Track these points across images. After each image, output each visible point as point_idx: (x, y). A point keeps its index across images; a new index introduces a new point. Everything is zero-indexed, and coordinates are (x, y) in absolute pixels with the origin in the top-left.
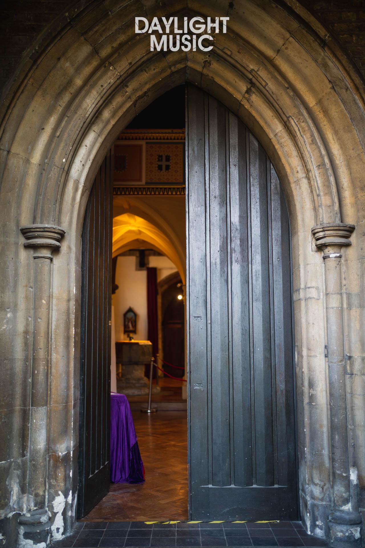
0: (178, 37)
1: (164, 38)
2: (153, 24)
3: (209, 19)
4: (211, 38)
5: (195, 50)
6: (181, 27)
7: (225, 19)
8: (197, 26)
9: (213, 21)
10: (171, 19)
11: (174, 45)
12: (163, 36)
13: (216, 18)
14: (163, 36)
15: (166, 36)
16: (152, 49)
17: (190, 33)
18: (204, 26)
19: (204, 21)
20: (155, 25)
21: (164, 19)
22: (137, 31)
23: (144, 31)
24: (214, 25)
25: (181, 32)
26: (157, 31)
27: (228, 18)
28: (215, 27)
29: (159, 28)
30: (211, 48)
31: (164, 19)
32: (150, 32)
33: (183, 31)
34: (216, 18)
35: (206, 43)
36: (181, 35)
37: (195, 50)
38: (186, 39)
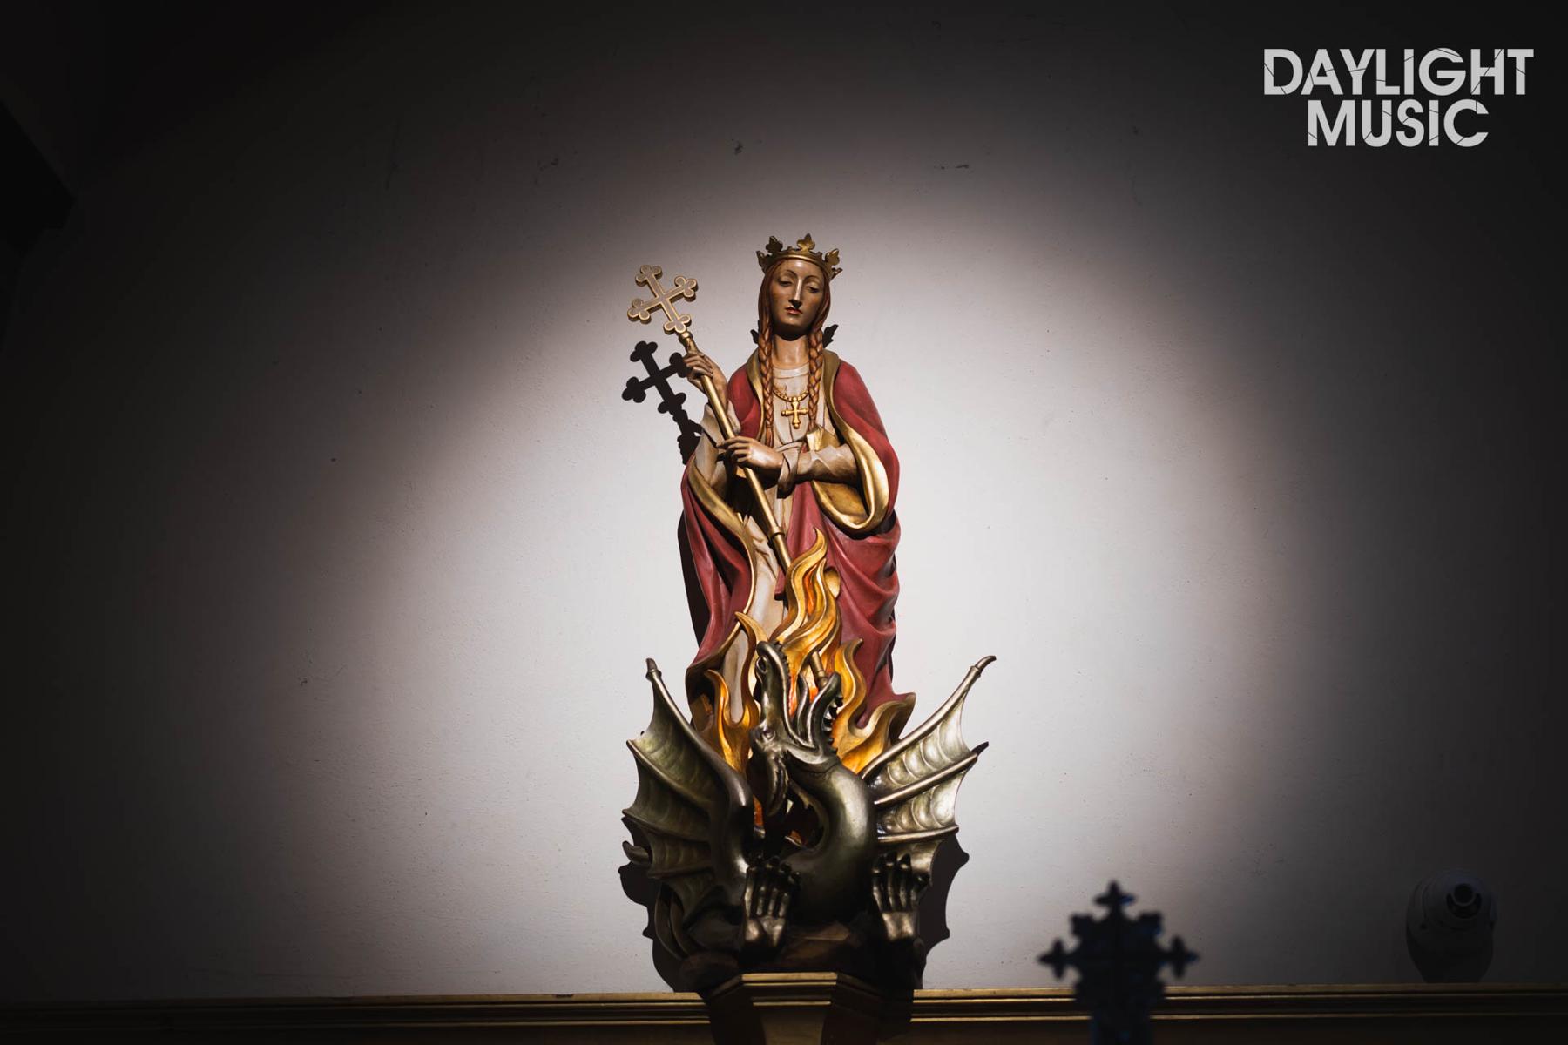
1: (1348, 108)
2: (1315, 69)
3: (1476, 54)
4: (1482, 110)
5: (1434, 142)
6: (1395, 77)
7: (1521, 55)
8: (1441, 74)
9: (1487, 61)
10: (1368, 53)
11: (1377, 131)
12: (1345, 103)
13: (1497, 51)
15: (1352, 103)
16: (1313, 141)
17: (1422, 95)
19: (1460, 60)
20: (1322, 72)
21: (1347, 54)
22: (1270, 89)
24: (1491, 72)
25: (1395, 90)
27: (1530, 53)
28: (1492, 79)
29: (1332, 80)
30: (1479, 138)
31: (1347, 54)
32: (1307, 90)
33: (1402, 90)
34: (1497, 51)
35: (1466, 123)
37: (1434, 142)
38: (1410, 112)
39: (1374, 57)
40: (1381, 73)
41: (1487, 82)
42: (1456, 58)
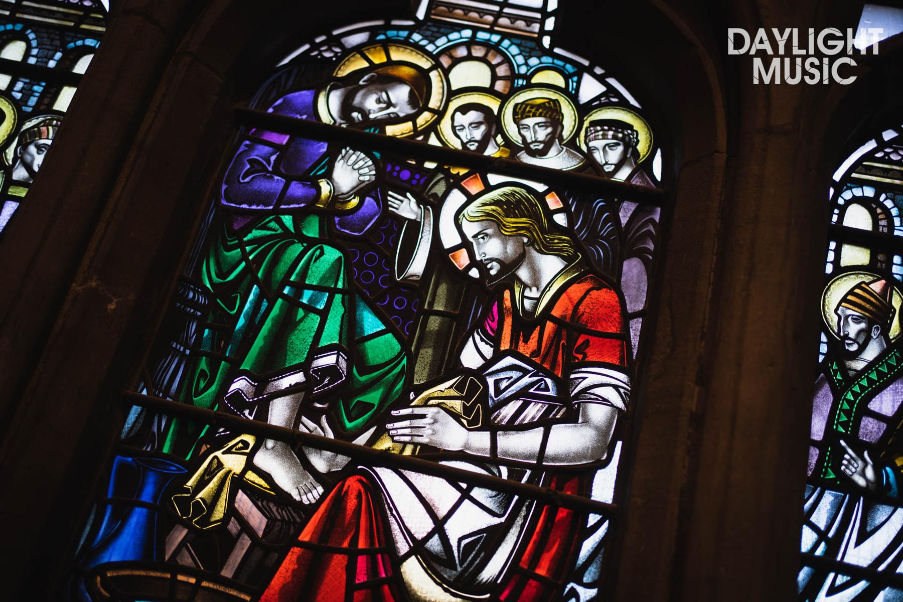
0: (799, 61)
1: (776, 62)
2: (757, 40)
3: (850, 31)
4: (853, 63)
5: (826, 82)
6: (803, 44)
8: (830, 43)
10: (788, 31)
11: (793, 75)
12: (774, 59)
15: (779, 59)
16: (756, 81)
17: (819, 55)
19: (841, 35)
20: (761, 42)
21: (775, 31)
22: (731, 51)
23: (743, 51)
25: (803, 52)
26: (765, 51)
29: (767, 46)
30: (852, 79)
31: (775, 31)
32: (753, 52)
33: (807, 52)
35: (844, 71)
36: (804, 58)
37: (826, 82)
38: (812, 65)
39: (791, 33)
40: (795, 42)
42: (838, 33)
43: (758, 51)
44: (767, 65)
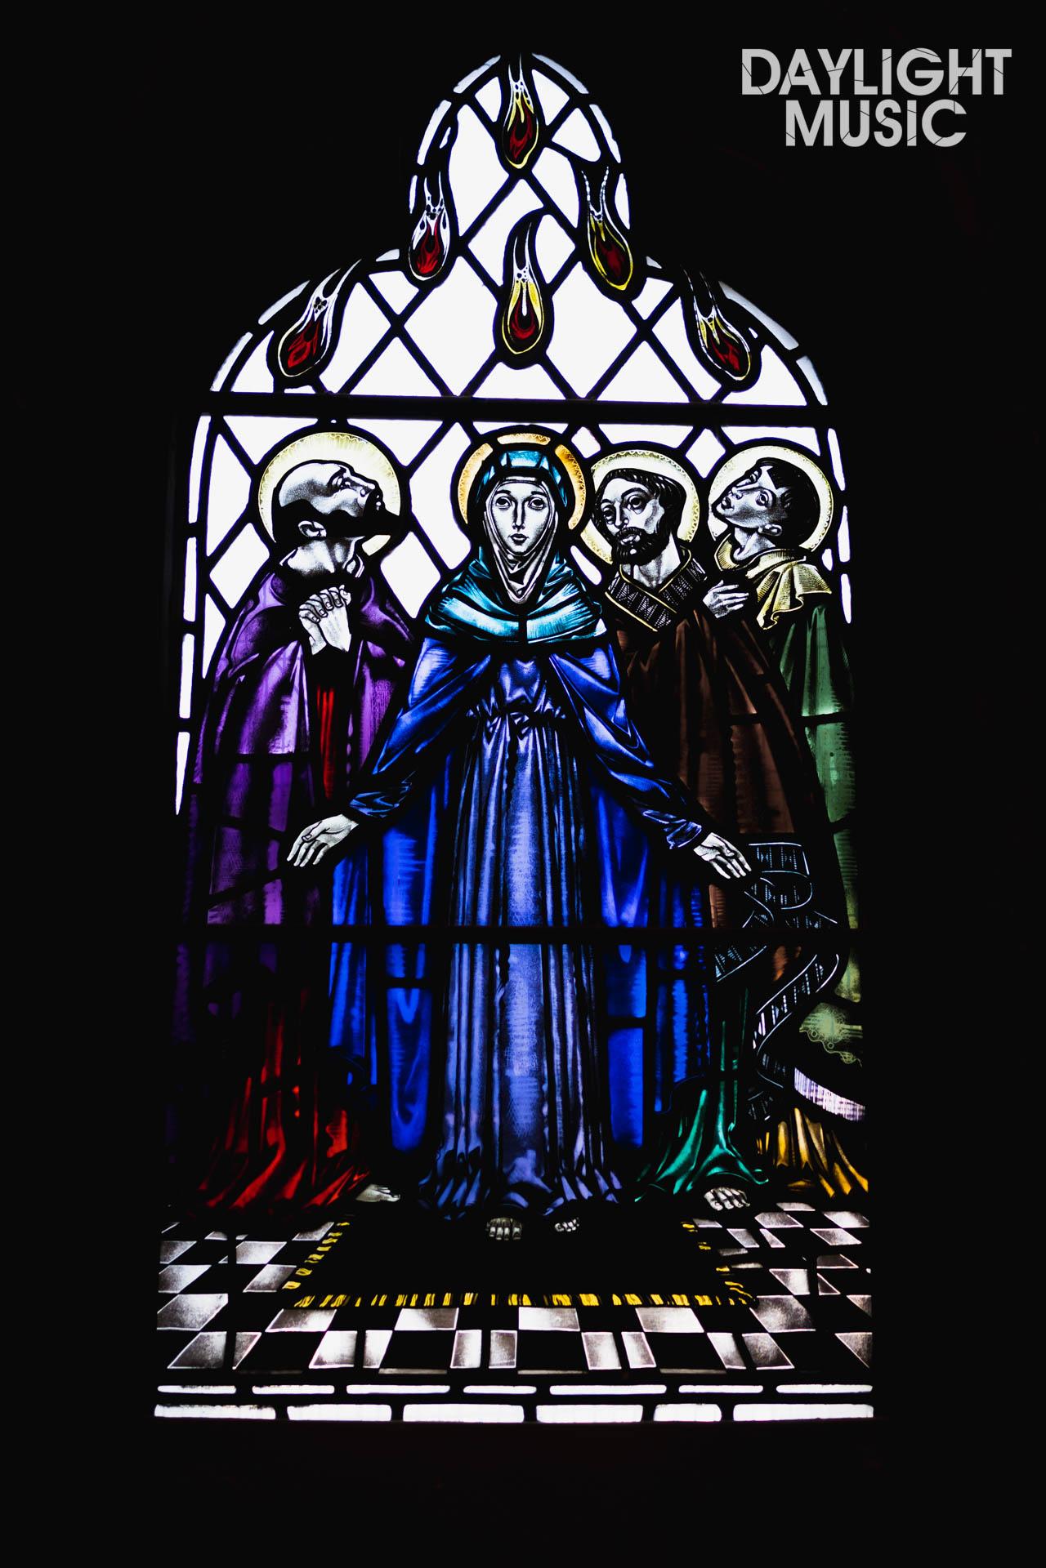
0: (865, 106)
1: (825, 108)
2: (793, 69)
3: (954, 54)
4: (959, 110)
5: (912, 142)
6: (873, 77)
7: (999, 55)
8: (919, 74)
9: (966, 61)
10: (845, 54)
11: (855, 131)
12: (823, 103)
13: (975, 51)
14: (823, 103)
15: (830, 103)
16: (790, 142)
17: (899, 95)
18: (941, 73)
19: (938, 60)
20: (800, 73)
21: (824, 54)
22: (748, 88)
23: (767, 89)
24: (969, 72)
25: (873, 90)
26: (806, 88)
27: (1008, 53)
28: (970, 78)
29: (810, 81)
30: (957, 138)
31: (824, 54)
32: (785, 90)
33: (880, 90)
34: (975, 51)
35: (944, 123)
36: (874, 101)
37: (912, 142)
38: (888, 113)
39: (852, 55)
41: (965, 82)
42: (934, 58)
43: (793, 88)
44: (809, 113)
